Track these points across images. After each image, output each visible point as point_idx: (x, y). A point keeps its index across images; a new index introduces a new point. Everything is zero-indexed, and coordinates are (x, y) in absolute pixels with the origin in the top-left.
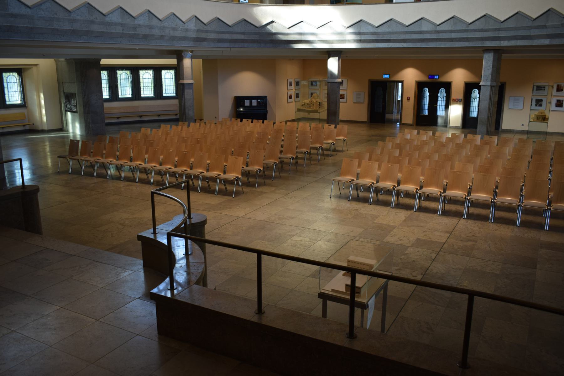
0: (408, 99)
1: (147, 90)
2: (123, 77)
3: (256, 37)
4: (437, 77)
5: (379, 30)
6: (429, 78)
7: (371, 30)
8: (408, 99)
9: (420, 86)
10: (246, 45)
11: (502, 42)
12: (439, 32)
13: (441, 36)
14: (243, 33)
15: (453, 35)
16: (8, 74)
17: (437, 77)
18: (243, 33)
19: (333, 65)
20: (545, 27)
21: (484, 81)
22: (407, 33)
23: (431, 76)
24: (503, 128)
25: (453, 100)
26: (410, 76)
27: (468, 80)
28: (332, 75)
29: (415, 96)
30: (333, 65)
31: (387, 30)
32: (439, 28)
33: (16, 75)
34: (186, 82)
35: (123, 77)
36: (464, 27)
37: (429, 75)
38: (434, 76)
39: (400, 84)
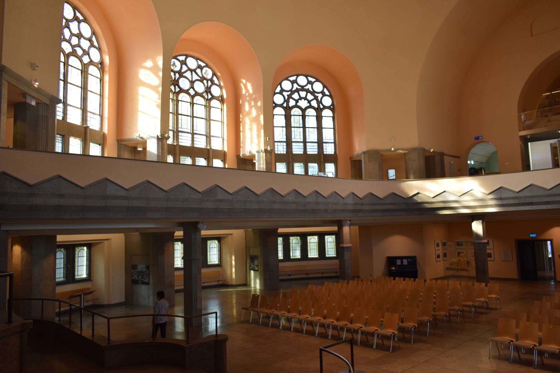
2: (295, 242)
16: (211, 241)
19: (477, 227)
28: (477, 236)
30: (477, 227)
33: (216, 242)
34: (345, 245)
35: (295, 242)
39: (549, 242)
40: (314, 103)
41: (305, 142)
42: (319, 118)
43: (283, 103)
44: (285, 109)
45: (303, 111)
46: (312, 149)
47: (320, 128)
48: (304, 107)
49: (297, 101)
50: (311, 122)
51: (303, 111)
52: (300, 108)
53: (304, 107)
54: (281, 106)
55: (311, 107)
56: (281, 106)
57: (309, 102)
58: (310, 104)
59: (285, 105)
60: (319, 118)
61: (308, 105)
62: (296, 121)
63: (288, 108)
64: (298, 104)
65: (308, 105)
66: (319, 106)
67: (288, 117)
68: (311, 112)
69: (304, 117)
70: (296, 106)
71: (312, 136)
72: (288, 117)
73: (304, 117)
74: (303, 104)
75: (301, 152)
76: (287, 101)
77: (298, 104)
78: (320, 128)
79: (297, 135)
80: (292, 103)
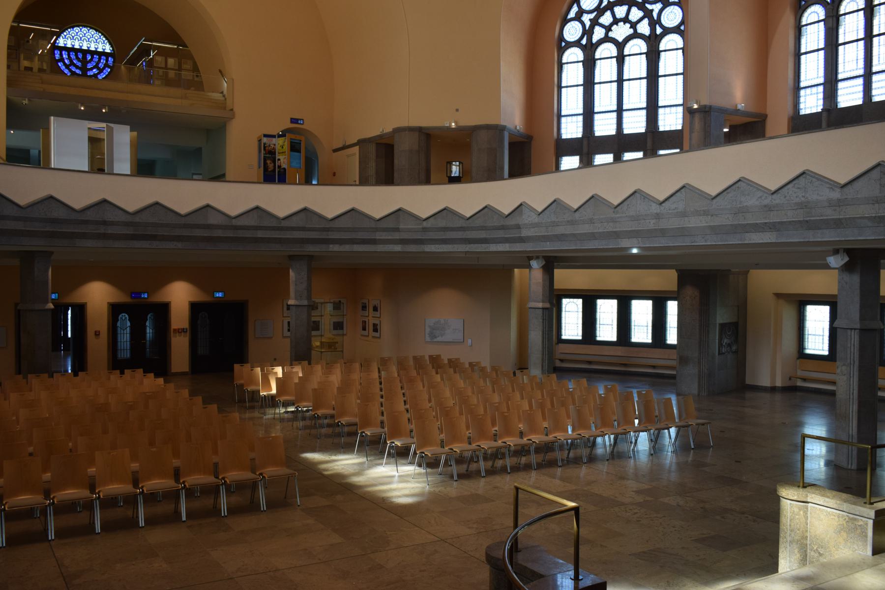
0: (97, 334)
1: (607, 331)
5: (137, 219)
6: (132, 298)
8: (97, 334)
9: (115, 309)
11: (331, 246)
12: (236, 228)
13: (241, 234)
15: (260, 234)
20: (397, 230)
21: (296, 299)
23: (136, 295)
24: (173, 371)
25: (175, 330)
26: (98, 295)
27: (113, 300)
29: (108, 329)
32: (235, 222)
36: (274, 224)
37: (132, 293)
38: (140, 293)
40: (644, 28)
41: (620, 111)
42: (653, 56)
43: (581, 38)
44: (583, 48)
45: (620, 46)
46: (635, 124)
47: (653, 77)
48: (620, 40)
49: (608, 29)
50: (636, 66)
51: (620, 46)
52: (614, 41)
53: (620, 40)
54: (577, 44)
55: (636, 35)
56: (577, 44)
57: (634, 25)
58: (635, 30)
59: (584, 42)
60: (653, 56)
61: (631, 31)
62: (605, 70)
63: (589, 46)
64: (611, 34)
65: (631, 31)
66: (653, 29)
67: (589, 64)
68: (638, 46)
69: (621, 59)
70: (607, 39)
71: (636, 94)
72: (589, 64)
73: (621, 59)
74: (621, 32)
75: (611, 131)
76: (588, 32)
77: (611, 34)
78: (653, 77)
79: (605, 98)
80: (599, 33)
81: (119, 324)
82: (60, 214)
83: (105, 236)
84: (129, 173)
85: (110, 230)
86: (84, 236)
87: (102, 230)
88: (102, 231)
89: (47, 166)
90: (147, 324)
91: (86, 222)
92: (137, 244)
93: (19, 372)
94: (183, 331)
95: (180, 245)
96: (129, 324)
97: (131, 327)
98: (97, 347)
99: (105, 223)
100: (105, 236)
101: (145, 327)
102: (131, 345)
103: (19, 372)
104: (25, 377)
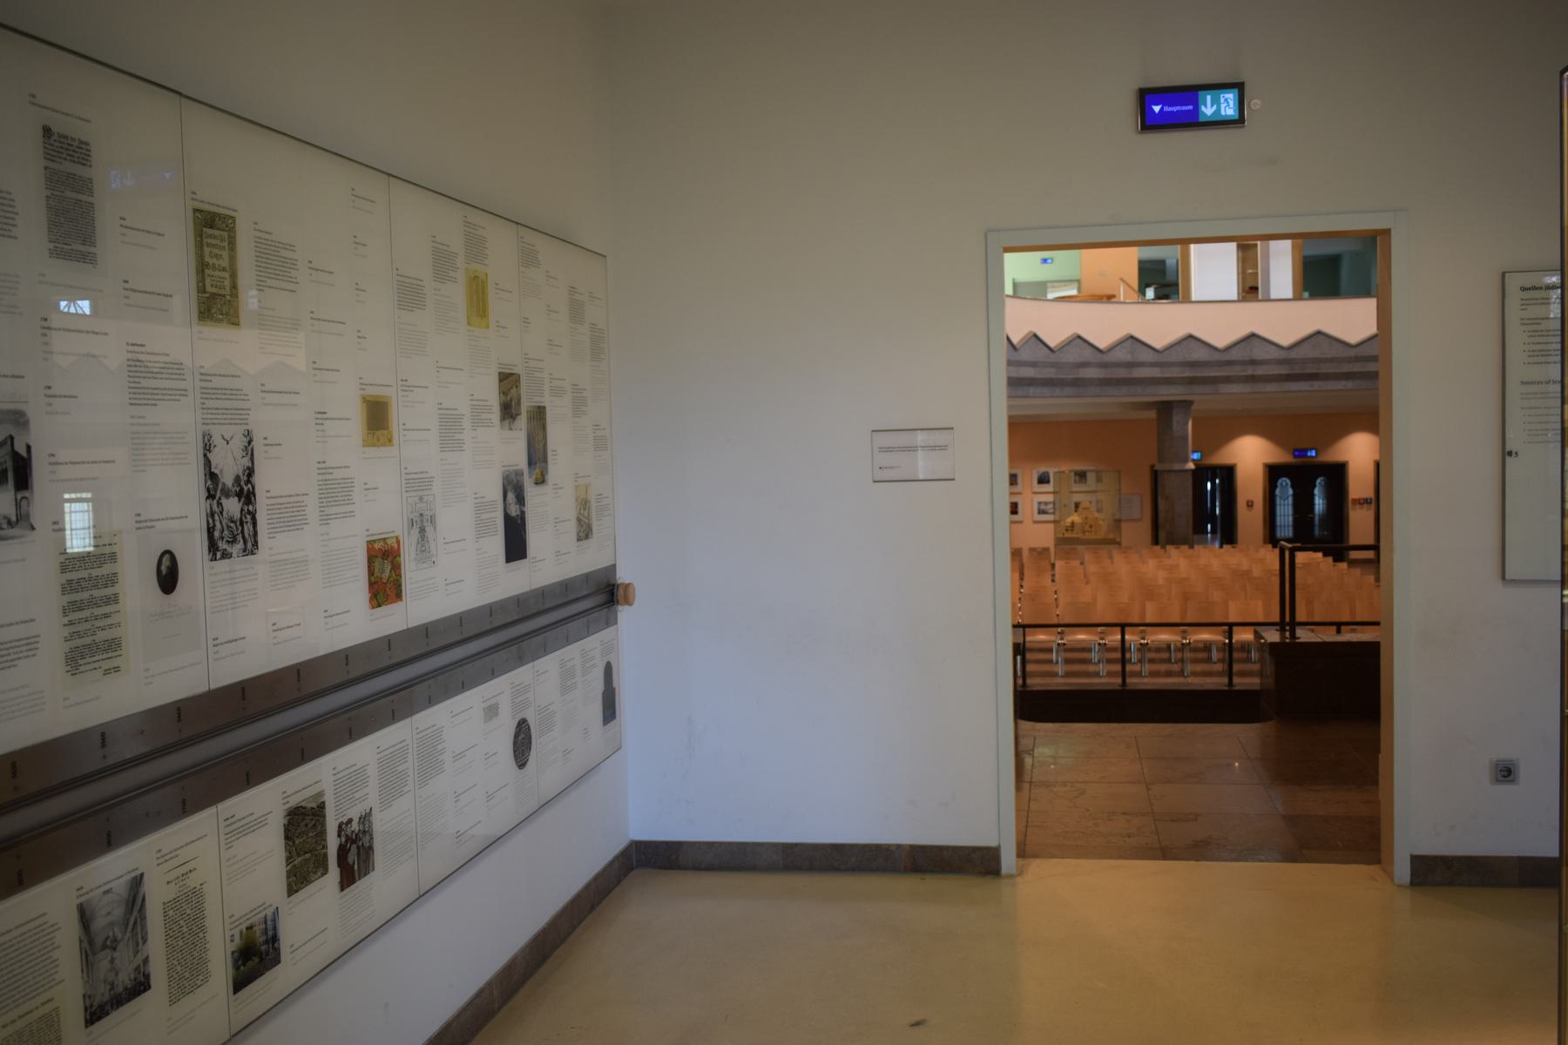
3: (1049, 373)
4: (1313, 453)
5: (1293, 355)
7: (1274, 354)
8: (1250, 505)
9: (1274, 472)
10: (1032, 390)
14: (1034, 365)
17: (1313, 453)
18: (1034, 365)
22: (1357, 359)
23: (1300, 452)
25: (1355, 501)
26: (1250, 454)
31: (1316, 354)
38: (1306, 450)
81: (1278, 492)
82: (1200, 355)
83: (1253, 379)
84: (1290, 295)
85: (1260, 371)
86: (1228, 380)
87: (1250, 371)
88: (1250, 372)
89: (1187, 300)
90: (1316, 491)
91: (1230, 363)
92: (1294, 386)
93: (1156, 541)
94: (1366, 501)
95: (1349, 384)
96: (1291, 491)
97: (1295, 496)
98: (1250, 520)
99: (1253, 362)
100: (1253, 379)
101: (1312, 496)
102: (1295, 521)
103: (1156, 541)
104: (1163, 547)
